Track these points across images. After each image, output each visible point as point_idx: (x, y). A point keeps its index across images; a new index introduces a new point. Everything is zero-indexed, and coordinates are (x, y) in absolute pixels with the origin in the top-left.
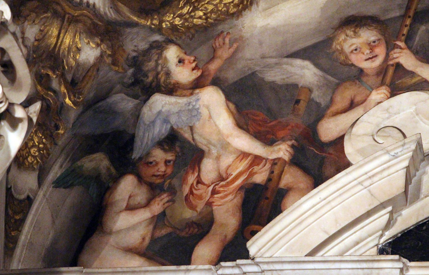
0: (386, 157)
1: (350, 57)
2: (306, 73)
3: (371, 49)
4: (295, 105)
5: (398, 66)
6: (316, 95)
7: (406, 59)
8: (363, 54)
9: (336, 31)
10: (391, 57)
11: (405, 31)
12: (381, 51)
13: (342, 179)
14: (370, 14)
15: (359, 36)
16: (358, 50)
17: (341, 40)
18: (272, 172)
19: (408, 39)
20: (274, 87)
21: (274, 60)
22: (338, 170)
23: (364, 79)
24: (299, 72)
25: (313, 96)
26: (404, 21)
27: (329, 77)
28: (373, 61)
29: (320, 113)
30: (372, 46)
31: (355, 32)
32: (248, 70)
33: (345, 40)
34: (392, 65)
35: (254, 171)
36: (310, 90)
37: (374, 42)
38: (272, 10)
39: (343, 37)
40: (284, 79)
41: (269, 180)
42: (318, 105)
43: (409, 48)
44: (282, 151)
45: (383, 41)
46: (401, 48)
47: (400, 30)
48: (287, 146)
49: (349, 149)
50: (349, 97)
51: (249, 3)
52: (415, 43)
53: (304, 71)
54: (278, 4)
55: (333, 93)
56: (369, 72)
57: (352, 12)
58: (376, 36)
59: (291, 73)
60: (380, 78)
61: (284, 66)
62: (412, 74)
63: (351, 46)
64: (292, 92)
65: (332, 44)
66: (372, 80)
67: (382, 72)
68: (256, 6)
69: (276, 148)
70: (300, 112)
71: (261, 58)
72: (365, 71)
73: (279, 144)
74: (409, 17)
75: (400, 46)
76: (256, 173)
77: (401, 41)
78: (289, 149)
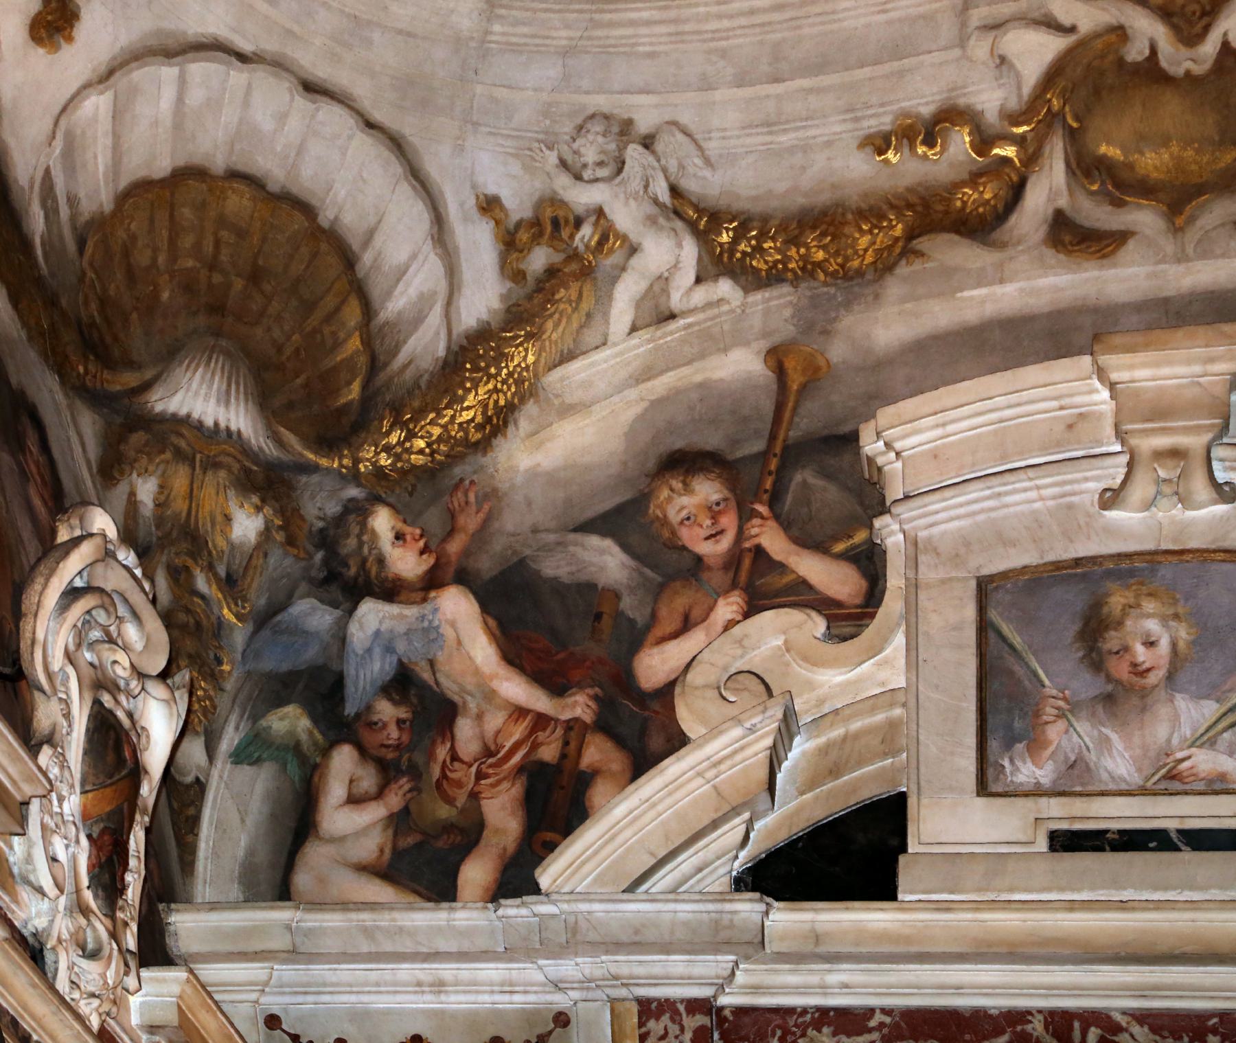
1: (679, 534)
2: (607, 561)
3: (713, 518)
5: (759, 551)
6: (627, 604)
7: (773, 541)
9: (653, 480)
11: (768, 485)
12: (729, 521)
14: (708, 448)
16: (693, 518)
17: (662, 498)
18: (566, 743)
19: (775, 500)
20: (559, 588)
23: (705, 576)
26: (766, 463)
28: (717, 542)
29: (636, 638)
31: (685, 484)
33: (669, 500)
34: (750, 550)
36: (617, 596)
37: (718, 504)
40: (573, 574)
41: (563, 756)
42: (632, 622)
43: (777, 517)
44: (579, 706)
45: (733, 504)
46: (763, 518)
47: (761, 481)
50: (681, 610)
52: (786, 508)
55: (656, 601)
56: (710, 561)
57: (679, 444)
58: (721, 491)
59: (584, 562)
60: (731, 574)
61: (571, 548)
62: (781, 567)
64: (589, 598)
65: (648, 507)
66: (718, 578)
67: (733, 560)
69: (570, 700)
72: (706, 559)
74: (775, 455)
76: (542, 744)
77: (761, 502)
78: (590, 703)
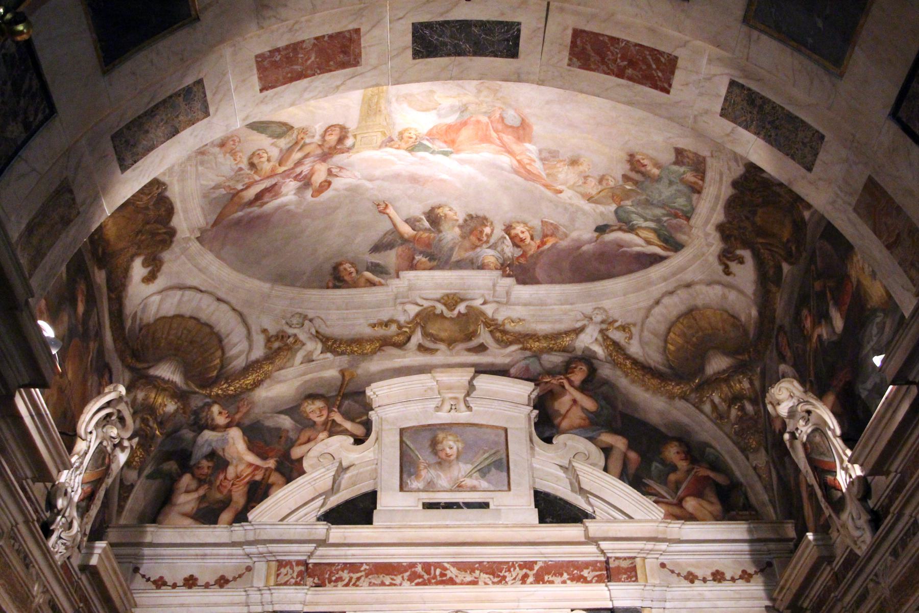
0: (323, 470)
2: (286, 422)
5: (333, 421)
7: (338, 418)
12: (325, 413)
13: (300, 480)
19: (339, 407)
20: (269, 429)
22: (300, 475)
29: (292, 444)
30: (321, 410)
36: (288, 431)
41: (263, 479)
43: (339, 412)
44: (271, 463)
49: (306, 465)
57: (311, 392)
62: (340, 425)
64: (278, 432)
66: (320, 428)
67: (325, 423)
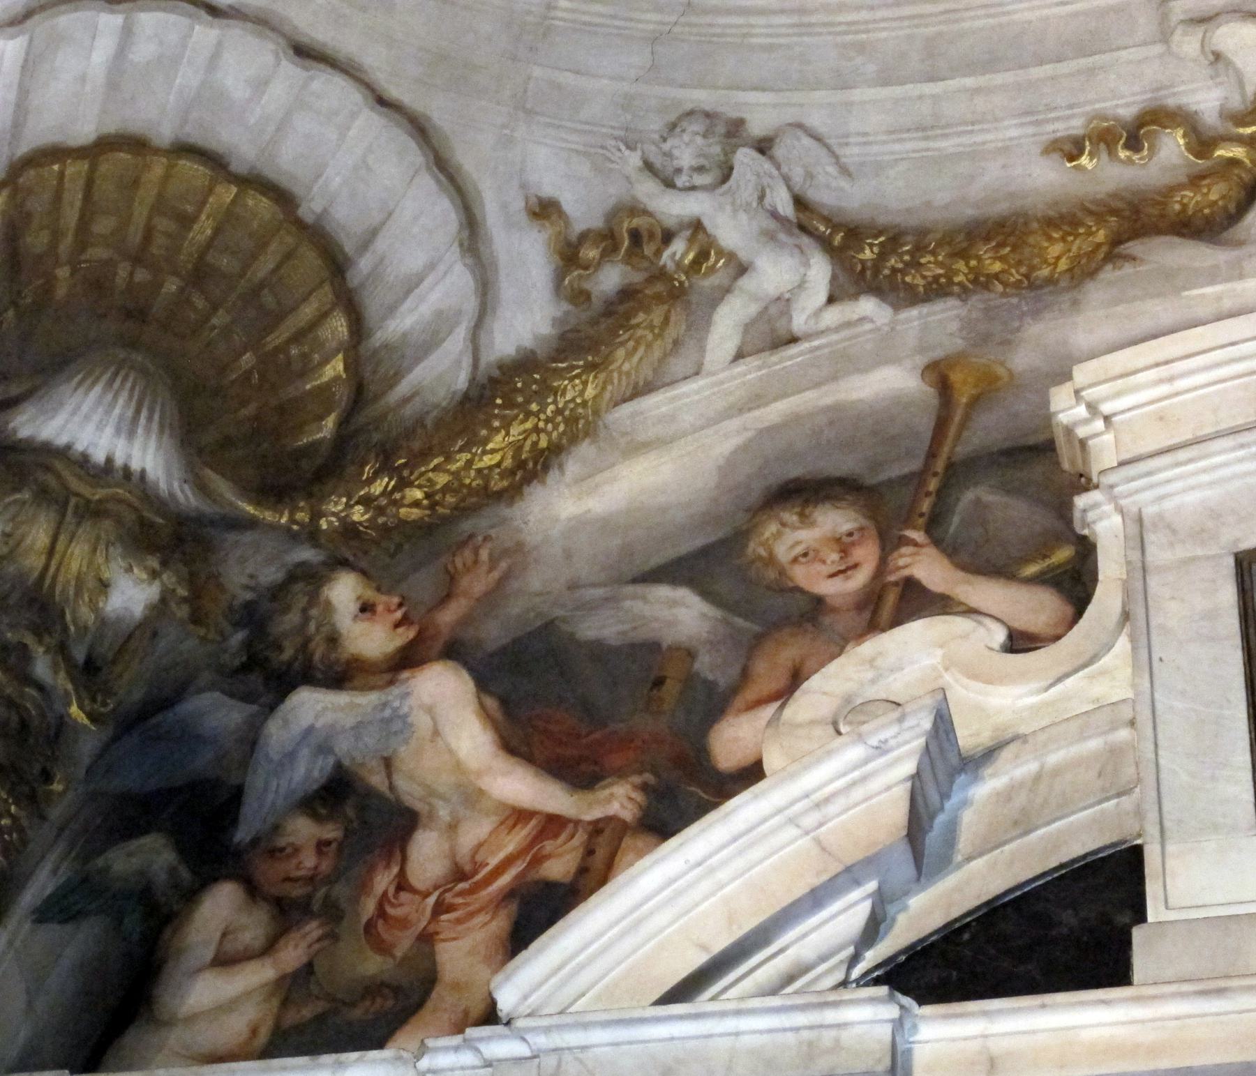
2: (682, 614)
4: (651, 689)
6: (704, 664)
8: (824, 562)
9: (754, 516)
10: (891, 565)
11: (926, 506)
12: (867, 555)
14: (838, 474)
15: (812, 524)
16: (811, 554)
17: (767, 534)
18: (590, 852)
19: (934, 525)
20: (599, 652)
21: (600, 592)
23: (827, 620)
24: (666, 613)
25: (697, 666)
27: (740, 622)
28: (848, 578)
29: (715, 704)
30: (843, 545)
31: (802, 515)
32: (536, 616)
33: (778, 535)
34: (896, 584)
35: (545, 852)
37: (850, 534)
38: (598, 478)
39: (772, 528)
42: (710, 686)
43: (937, 542)
46: (916, 544)
48: (629, 786)
50: (790, 664)
51: (539, 467)
52: (952, 529)
53: (674, 611)
54: (613, 465)
55: (749, 658)
56: (837, 602)
57: (795, 471)
58: (855, 520)
60: (867, 615)
61: (628, 604)
63: (793, 547)
68: (557, 472)
69: (603, 794)
70: (666, 707)
71: (569, 588)
72: (828, 600)
73: (611, 784)
75: (913, 540)
76: (548, 857)
77: (915, 528)
78: (634, 795)
